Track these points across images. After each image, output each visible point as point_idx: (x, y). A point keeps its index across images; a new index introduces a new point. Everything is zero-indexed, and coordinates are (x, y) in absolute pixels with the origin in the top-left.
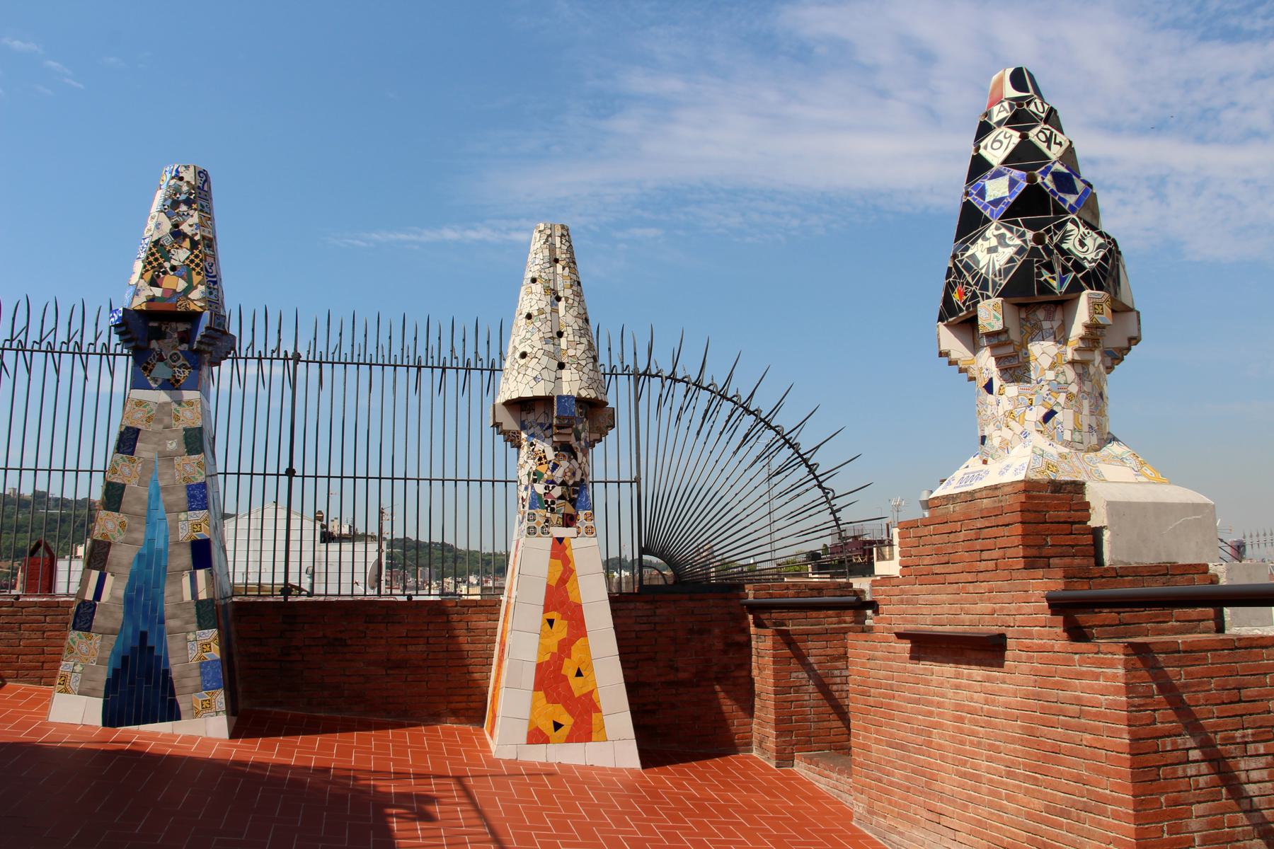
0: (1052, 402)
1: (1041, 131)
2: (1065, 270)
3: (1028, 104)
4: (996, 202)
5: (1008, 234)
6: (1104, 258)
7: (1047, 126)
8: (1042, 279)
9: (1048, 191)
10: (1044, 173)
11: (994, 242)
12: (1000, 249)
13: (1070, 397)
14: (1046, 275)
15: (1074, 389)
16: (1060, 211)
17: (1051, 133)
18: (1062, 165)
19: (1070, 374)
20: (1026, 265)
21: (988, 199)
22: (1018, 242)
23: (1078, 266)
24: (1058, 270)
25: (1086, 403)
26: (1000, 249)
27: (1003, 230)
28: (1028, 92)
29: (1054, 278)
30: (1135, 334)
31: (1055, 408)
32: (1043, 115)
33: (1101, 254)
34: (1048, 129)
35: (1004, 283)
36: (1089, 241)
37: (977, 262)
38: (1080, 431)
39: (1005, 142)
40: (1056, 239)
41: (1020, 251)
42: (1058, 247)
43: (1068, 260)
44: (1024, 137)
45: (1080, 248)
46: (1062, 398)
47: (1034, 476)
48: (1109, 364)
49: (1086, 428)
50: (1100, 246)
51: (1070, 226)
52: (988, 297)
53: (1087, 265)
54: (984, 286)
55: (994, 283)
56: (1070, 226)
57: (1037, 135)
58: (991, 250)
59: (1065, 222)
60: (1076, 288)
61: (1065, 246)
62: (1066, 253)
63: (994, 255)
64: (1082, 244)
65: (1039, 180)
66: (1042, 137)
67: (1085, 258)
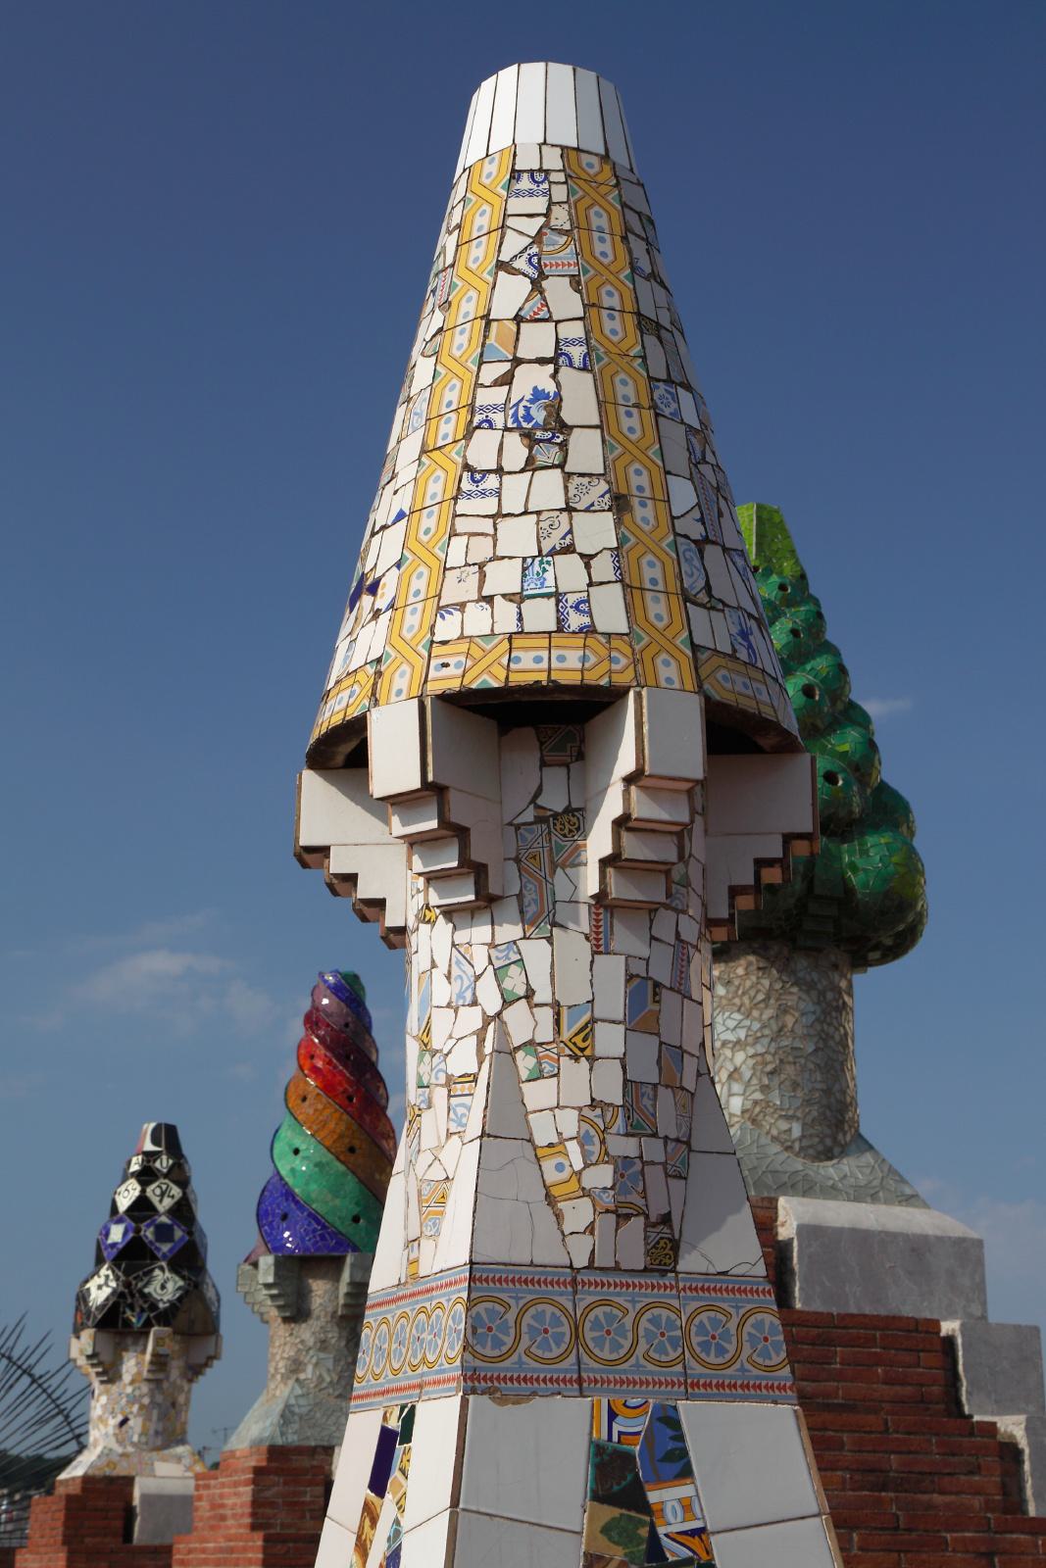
0: (128, 1410)
1: (158, 1186)
2: (143, 1310)
3: (155, 1161)
4: (114, 1245)
5: (111, 1277)
6: (180, 1299)
7: (167, 1181)
8: (125, 1316)
9: (146, 1241)
10: (148, 1226)
11: (101, 1281)
12: (104, 1288)
13: (142, 1407)
14: (129, 1313)
15: (146, 1401)
16: (154, 1258)
17: (168, 1186)
18: (168, 1217)
19: (145, 1388)
20: (116, 1305)
21: (110, 1241)
22: (113, 1284)
23: (153, 1306)
24: (138, 1310)
25: (155, 1413)
26: (104, 1288)
27: (110, 1272)
28: (160, 1146)
29: (133, 1316)
30: (213, 1354)
31: (130, 1416)
32: (165, 1171)
33: (177, 1295)
34: (165, 1184)
35: (99, 1317)
36: (170, 1286)
37: (89, 1295)
38: (146, 1435)
39: (132, 1192)
40: (140, 1285)
41: (114, 1292)
42: (140, 1292)
43: (145, 1302)
44: (143, 1191)
45: (159, 1291)
46: (135, 1408)
47: (91, 1473)
48: (190, 1376)
49: (152, 1432)
50: (180, 1288)
51: (157, 1272)
52: (89, 1327)
53: (161, 1305)
54: (88, 1319)
55: (95, 1317)
56: (157, 1272)
57: (153, 1191)
58: (100, 1287)
59: (152, 1270)
60: (148, 1324)
61: (146, 1290)
62: (146, 1297)
63: (100, 1292)
64: (163, 1287)
65: (142, 1233)
66: (158, 1191)
67: (162, 1300)
